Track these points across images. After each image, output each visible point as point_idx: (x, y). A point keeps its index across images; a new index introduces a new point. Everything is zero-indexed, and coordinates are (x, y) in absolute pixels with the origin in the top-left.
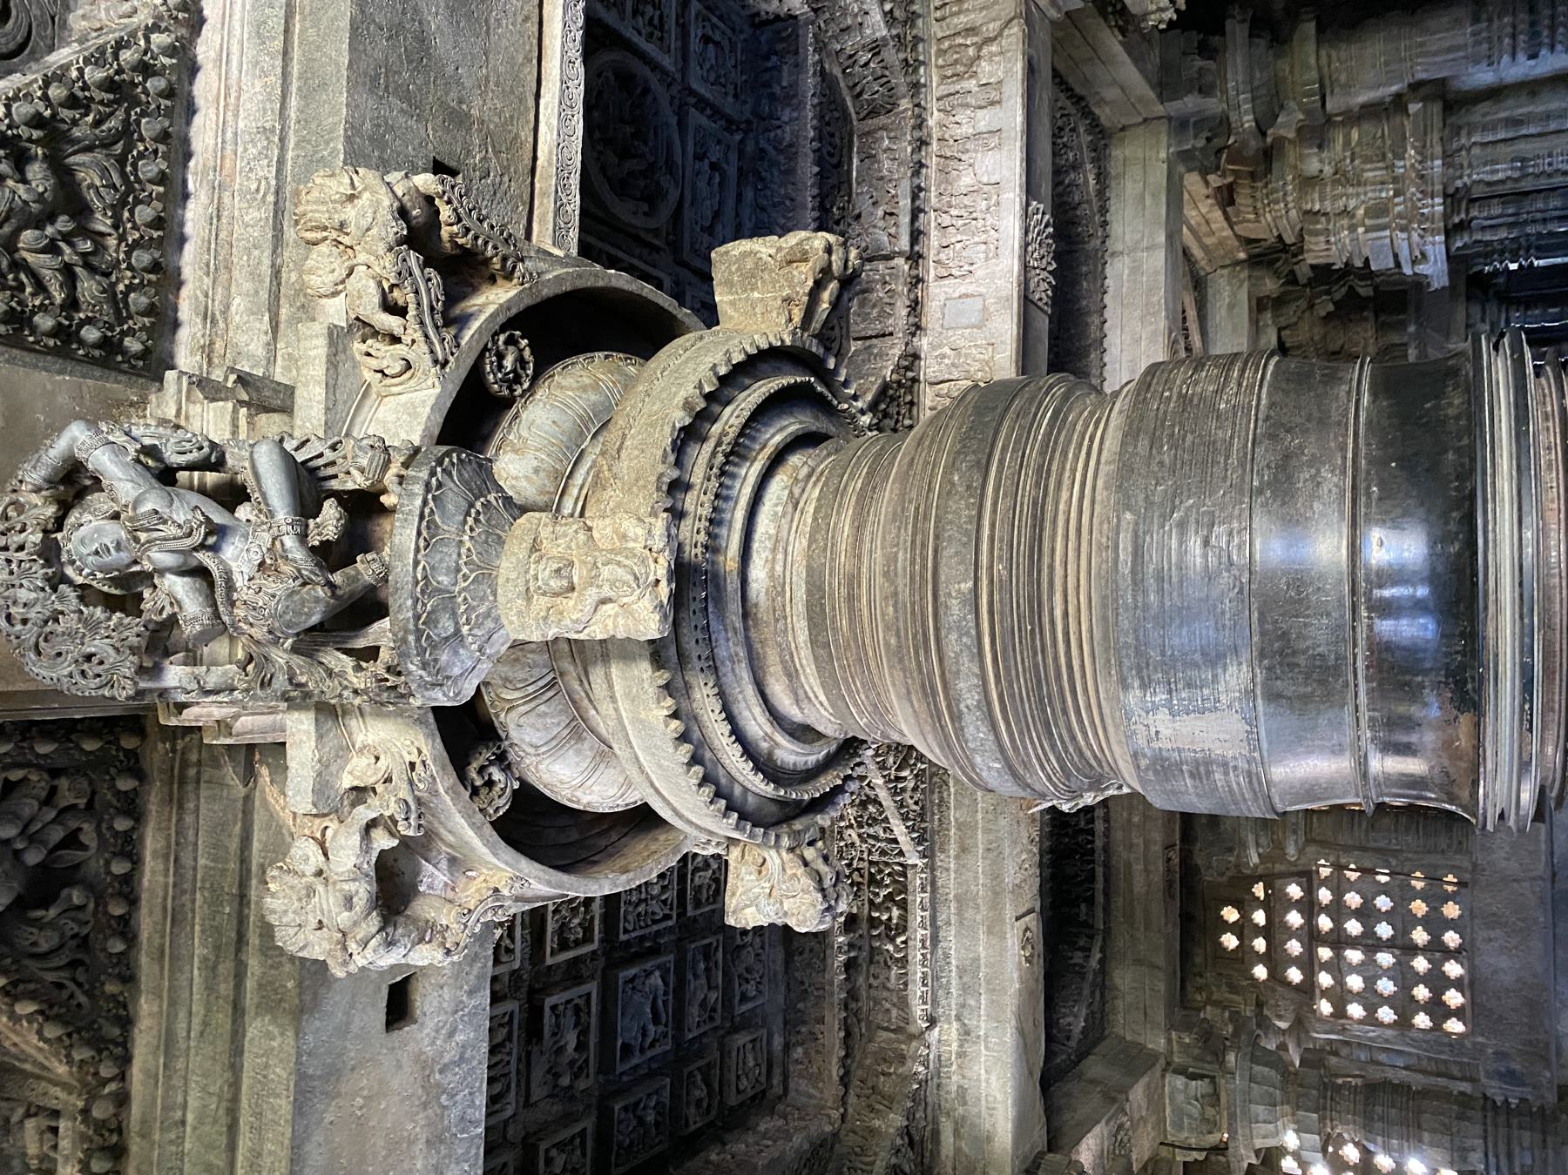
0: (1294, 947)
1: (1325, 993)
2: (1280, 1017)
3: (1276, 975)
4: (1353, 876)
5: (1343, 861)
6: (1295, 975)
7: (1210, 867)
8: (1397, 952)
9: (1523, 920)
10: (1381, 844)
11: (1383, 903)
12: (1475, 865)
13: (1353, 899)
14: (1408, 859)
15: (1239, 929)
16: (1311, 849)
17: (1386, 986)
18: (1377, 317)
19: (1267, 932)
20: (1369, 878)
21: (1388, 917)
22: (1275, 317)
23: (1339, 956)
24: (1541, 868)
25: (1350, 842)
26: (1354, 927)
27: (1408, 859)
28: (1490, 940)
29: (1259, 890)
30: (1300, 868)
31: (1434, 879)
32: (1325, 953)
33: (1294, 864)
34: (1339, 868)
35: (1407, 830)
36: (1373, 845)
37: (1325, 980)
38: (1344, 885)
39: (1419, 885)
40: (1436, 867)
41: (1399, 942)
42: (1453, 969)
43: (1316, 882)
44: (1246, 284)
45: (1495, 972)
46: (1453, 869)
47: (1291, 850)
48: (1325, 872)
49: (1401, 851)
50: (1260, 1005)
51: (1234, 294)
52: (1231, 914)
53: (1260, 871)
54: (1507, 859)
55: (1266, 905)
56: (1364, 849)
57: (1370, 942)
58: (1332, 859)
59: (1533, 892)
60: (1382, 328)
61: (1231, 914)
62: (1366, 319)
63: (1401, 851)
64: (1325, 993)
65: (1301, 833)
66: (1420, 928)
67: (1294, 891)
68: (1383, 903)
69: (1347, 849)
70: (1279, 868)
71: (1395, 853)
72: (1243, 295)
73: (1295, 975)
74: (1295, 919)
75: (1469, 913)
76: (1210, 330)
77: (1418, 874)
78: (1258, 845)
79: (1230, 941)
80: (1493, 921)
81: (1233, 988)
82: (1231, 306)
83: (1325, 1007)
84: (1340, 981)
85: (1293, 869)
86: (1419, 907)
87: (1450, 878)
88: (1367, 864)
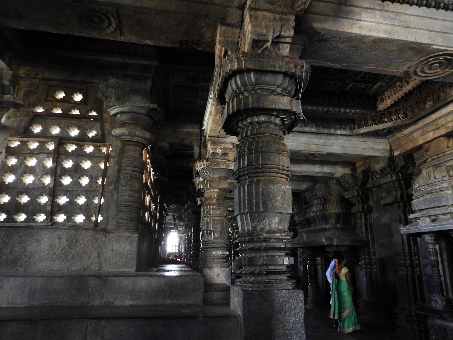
0: (56, 131)
1: (24, 143)
2: (8, 118)
3: (36, 118)
4: (102, 166)
5: (112, 160)
6: (37, 129)
7: (108, 87)
8: (51, 186)
9: (73, 257)
10: (122, 182)
11: (85, 181)
12: (109, 232)
13: (87, 165)
14: (112, 195)
15: (68, 100)
16: (118, 143)
17: (29, 180)
18: (342, 214)
19: (66, 115)
20: (101, 174)
21: (76, 184)
22: (348, 174)
23: (49, 154)
24: (108, 268)
25: (124, 165)
26: (69, 164)
27: (112, 195)
28: (60, 239)
29: (94, 114)
30: (107, 137)
31: (100, 209)
32: (51, 147)
33: (110, 133)
34: (107, 158)
35: (130, 196)
36: (122, 176)
37: (34, 145)
38: (95, 160)
39: (96, 201)
40: (107, 210)
41: (58, 188)
42: (41, 218)
43: (98, 144)
44: (382, 155)
45: (38, 241)
46: (106, 220)
47: (118, 131)
48: (104, 150)
49: (118, 192)
50: (16, 106)
51: (378, 150)
52: (78, 98)
53: (105, 115)
54: (113, 250)
55: (84, 117)
56: (119, 171)
57: (59, 172)
58: (112, 154)
59: (91, 264)
60: (338, 216)
61: (78, 98)
62: (342, 209)
63: (118, 192)
64: (24, 143)
65: (128, 138)
66: (68, 200)
67: (91, 134)
68: (85, 181)
69: (119, 163)
70: (107, 126)
71: (116, 188)
72: (378, 154)
73: (37, 129)
74: (74, 133)
75: (76, 227)
76: (365, 139)
77: (103, 200)
78: (121, 113)
79: (61, 95)
80: (72, 242)
81: (28, 94)
82: (373, 149)
83: (15, 144)
84: (32, 154)
85: (106, 133)
86: (82, 201)
87: (100, 218)
88: (109, 173)
